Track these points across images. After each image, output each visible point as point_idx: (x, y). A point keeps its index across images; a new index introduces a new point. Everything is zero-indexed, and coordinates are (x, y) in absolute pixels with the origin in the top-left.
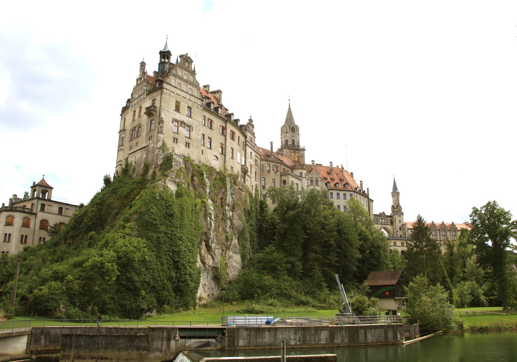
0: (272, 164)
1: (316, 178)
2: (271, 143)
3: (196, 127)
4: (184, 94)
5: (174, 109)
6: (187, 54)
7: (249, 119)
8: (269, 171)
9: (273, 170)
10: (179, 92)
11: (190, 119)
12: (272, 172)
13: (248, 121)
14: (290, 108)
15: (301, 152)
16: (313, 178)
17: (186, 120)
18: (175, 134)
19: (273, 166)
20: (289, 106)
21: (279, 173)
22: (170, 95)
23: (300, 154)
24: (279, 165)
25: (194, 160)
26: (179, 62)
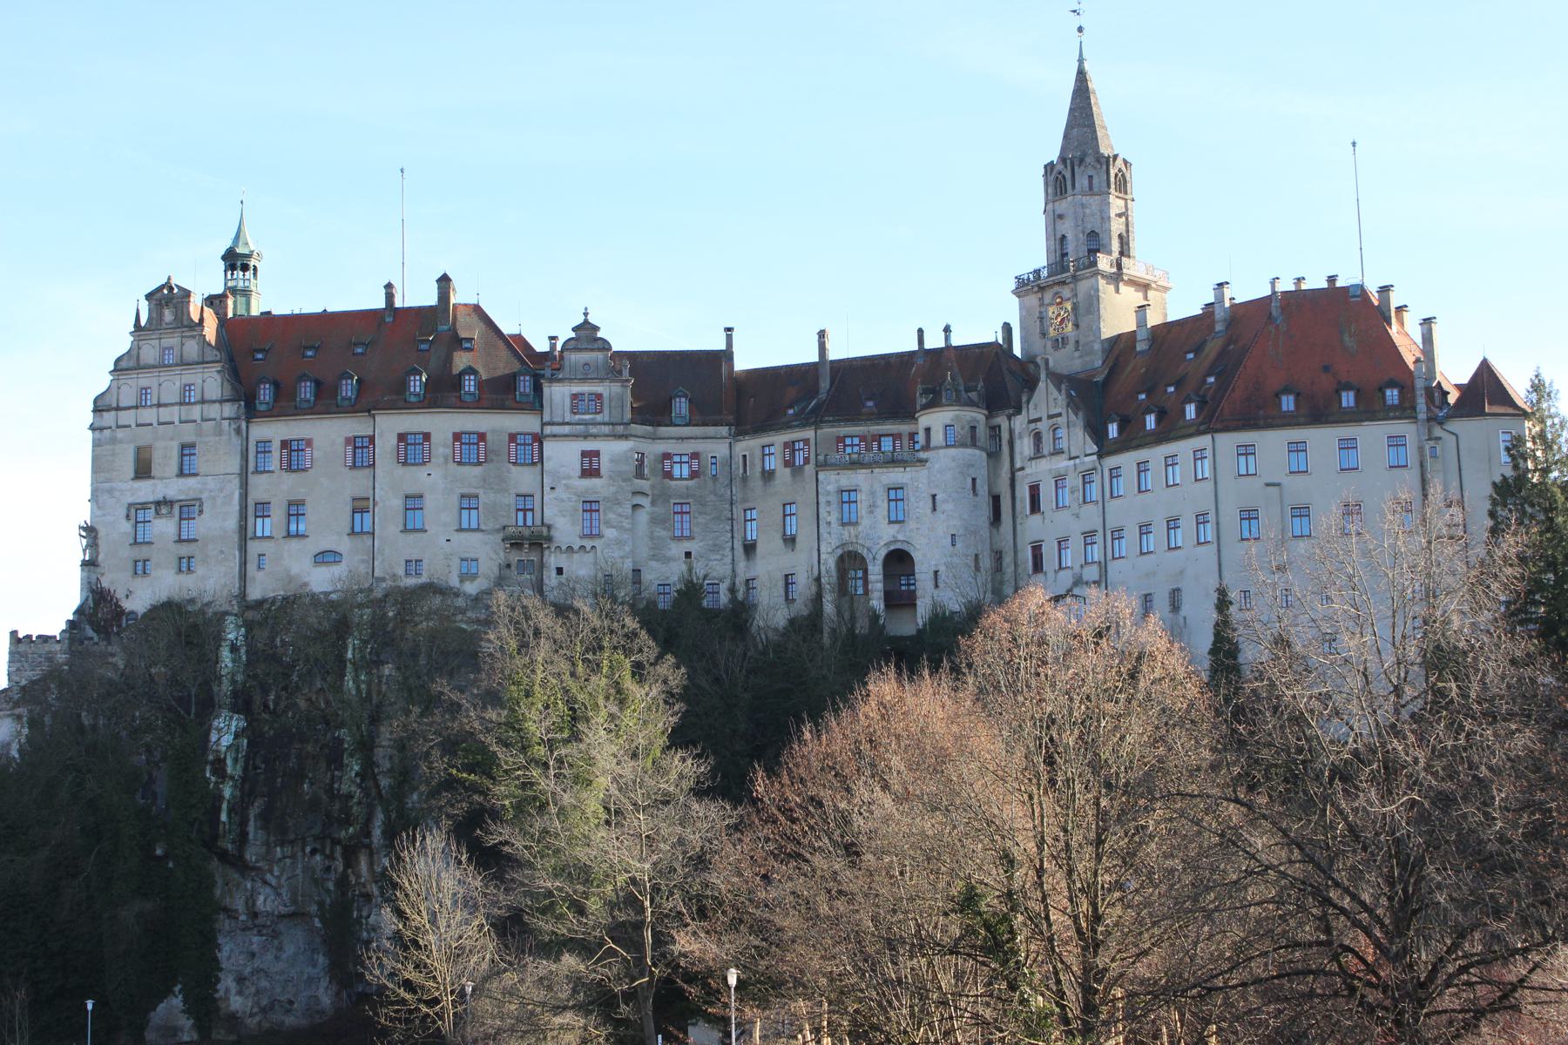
0: (779, 439)
1: (1050, 417)
2: (822, 334)
3: (214, 498)
4: (165, 414)
5: (132, 475)
6: (169, 278)
7: (580, 320)
8: (768, 476)
9: (787, 464)
10: (148, 415)
11: (191, 481)
12: (784, 474)
13: (573, 335)
14: (1081, 76)
15: (1083, 286)
16: (1039, 420)
17: (174, 488)
18: (136, 549)
19: (786, 445)
20: (1081, 61)
21: (809, 469)
22: (114, 441)
23: (1081, 297)
24: (809, 433)
25: (208, 604)
26: (143, 322)
